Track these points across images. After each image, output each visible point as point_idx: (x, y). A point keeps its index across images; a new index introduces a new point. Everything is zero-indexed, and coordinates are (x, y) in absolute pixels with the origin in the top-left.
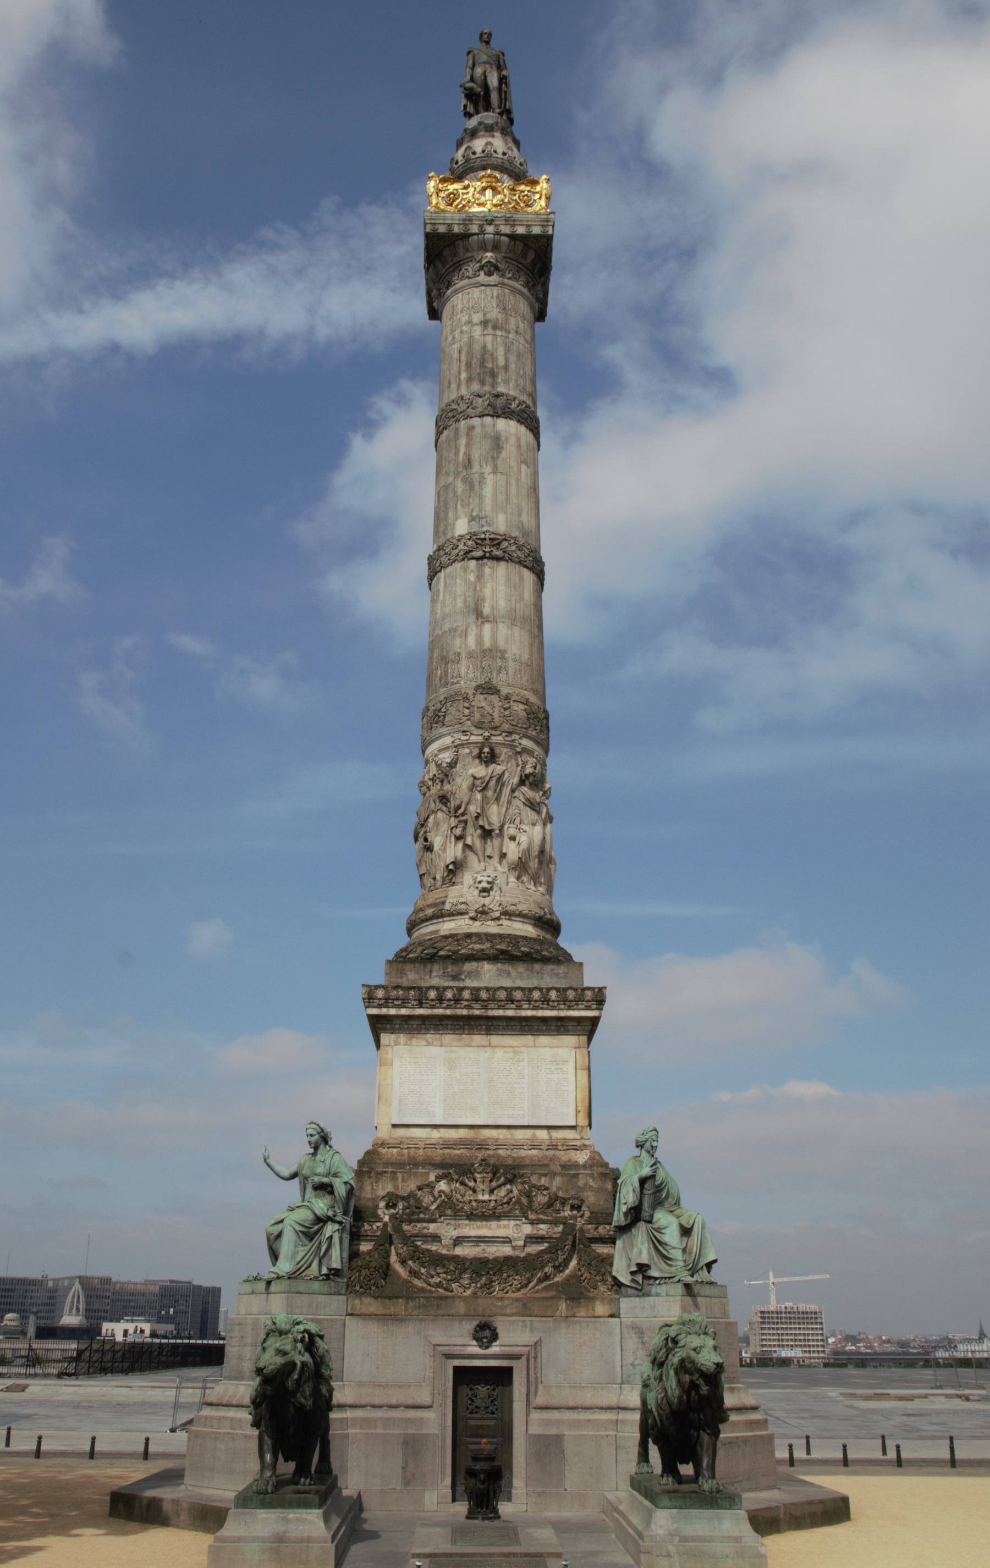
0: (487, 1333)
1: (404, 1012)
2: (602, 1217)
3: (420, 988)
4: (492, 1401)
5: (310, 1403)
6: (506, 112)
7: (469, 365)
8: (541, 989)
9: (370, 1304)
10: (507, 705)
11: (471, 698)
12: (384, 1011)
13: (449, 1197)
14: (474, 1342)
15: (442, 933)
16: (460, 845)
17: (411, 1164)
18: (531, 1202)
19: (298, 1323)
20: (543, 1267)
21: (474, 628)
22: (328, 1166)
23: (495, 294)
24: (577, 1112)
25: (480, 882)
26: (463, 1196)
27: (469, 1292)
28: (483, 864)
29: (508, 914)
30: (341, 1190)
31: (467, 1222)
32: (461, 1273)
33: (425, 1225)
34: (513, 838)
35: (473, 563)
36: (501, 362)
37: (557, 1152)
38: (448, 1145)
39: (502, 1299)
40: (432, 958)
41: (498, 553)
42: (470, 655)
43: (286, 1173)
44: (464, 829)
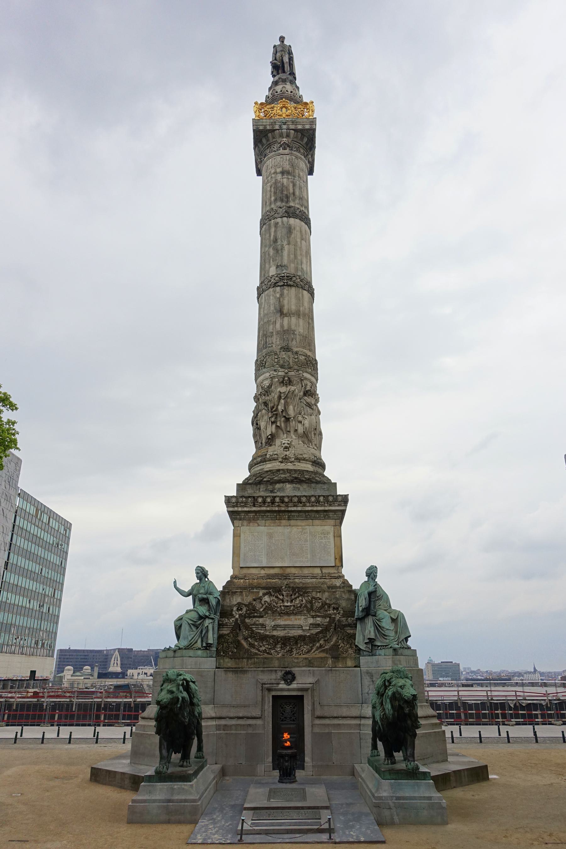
0: (290, 676)
1: (245, 509)
2: (350, 613)
3: (254, 497)
4: (293, 714)
5: (187, 720)
6: (292, 74)
7: (275, 193)
8: (315, 496)
9: (228, 662)
10: (296, 357)
11: (278, 354)
12: (236, 509)
13: (270, 604)
14: (283, 682)
15: (265, 470)
16: (274, 426)
17: (250, 588)
18: (312, 606)
19: (180, 675)
20: (319, 641)
21: (279, 320)
22: (206, 589)
23: (288, 159)
24: (336, 559)
25: (284, 444)
26: (277, 604)
27: (280, 655)
28: (285, 435)
29: (298, 460)
30: (213, 602)
31: (279, 617)
32: (276, 645)
33: (257, 619)
34: (301, 422)
35: (278, 289)
37: (325, 580)
38: (270, 576)
39: (297, 658)
40: (260, 483)
41: (291, 283)
42: (278, 333)
43: (186, 594)
44: (276, 418)
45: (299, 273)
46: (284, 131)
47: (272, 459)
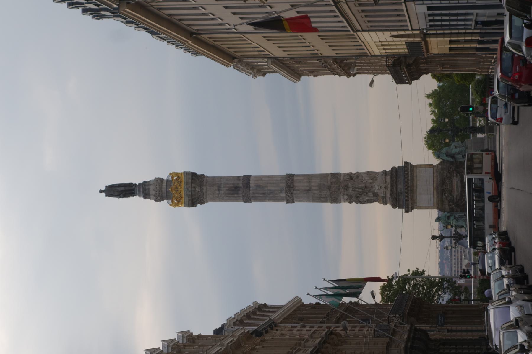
2: (452, 163)
7: (232, 194)
29: (386, 182)
35: (295, 192)
36: (232, 185)
45: (284, 181)
46: (192, 189)
47: (386, 194)
